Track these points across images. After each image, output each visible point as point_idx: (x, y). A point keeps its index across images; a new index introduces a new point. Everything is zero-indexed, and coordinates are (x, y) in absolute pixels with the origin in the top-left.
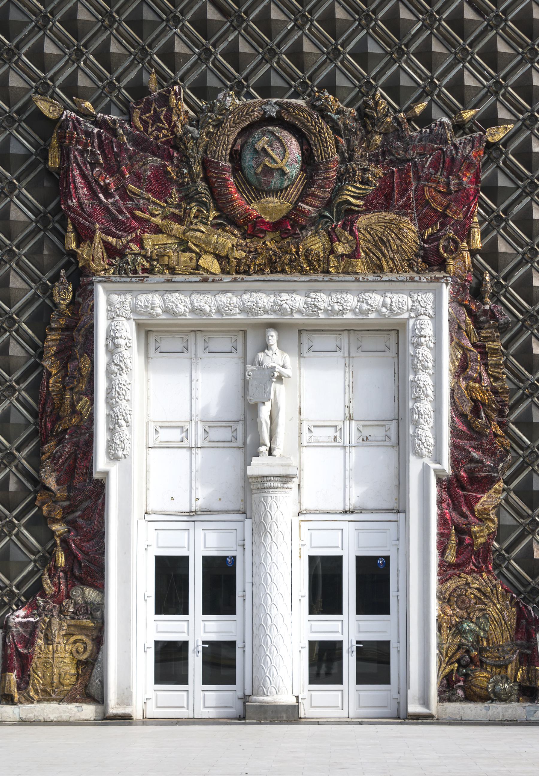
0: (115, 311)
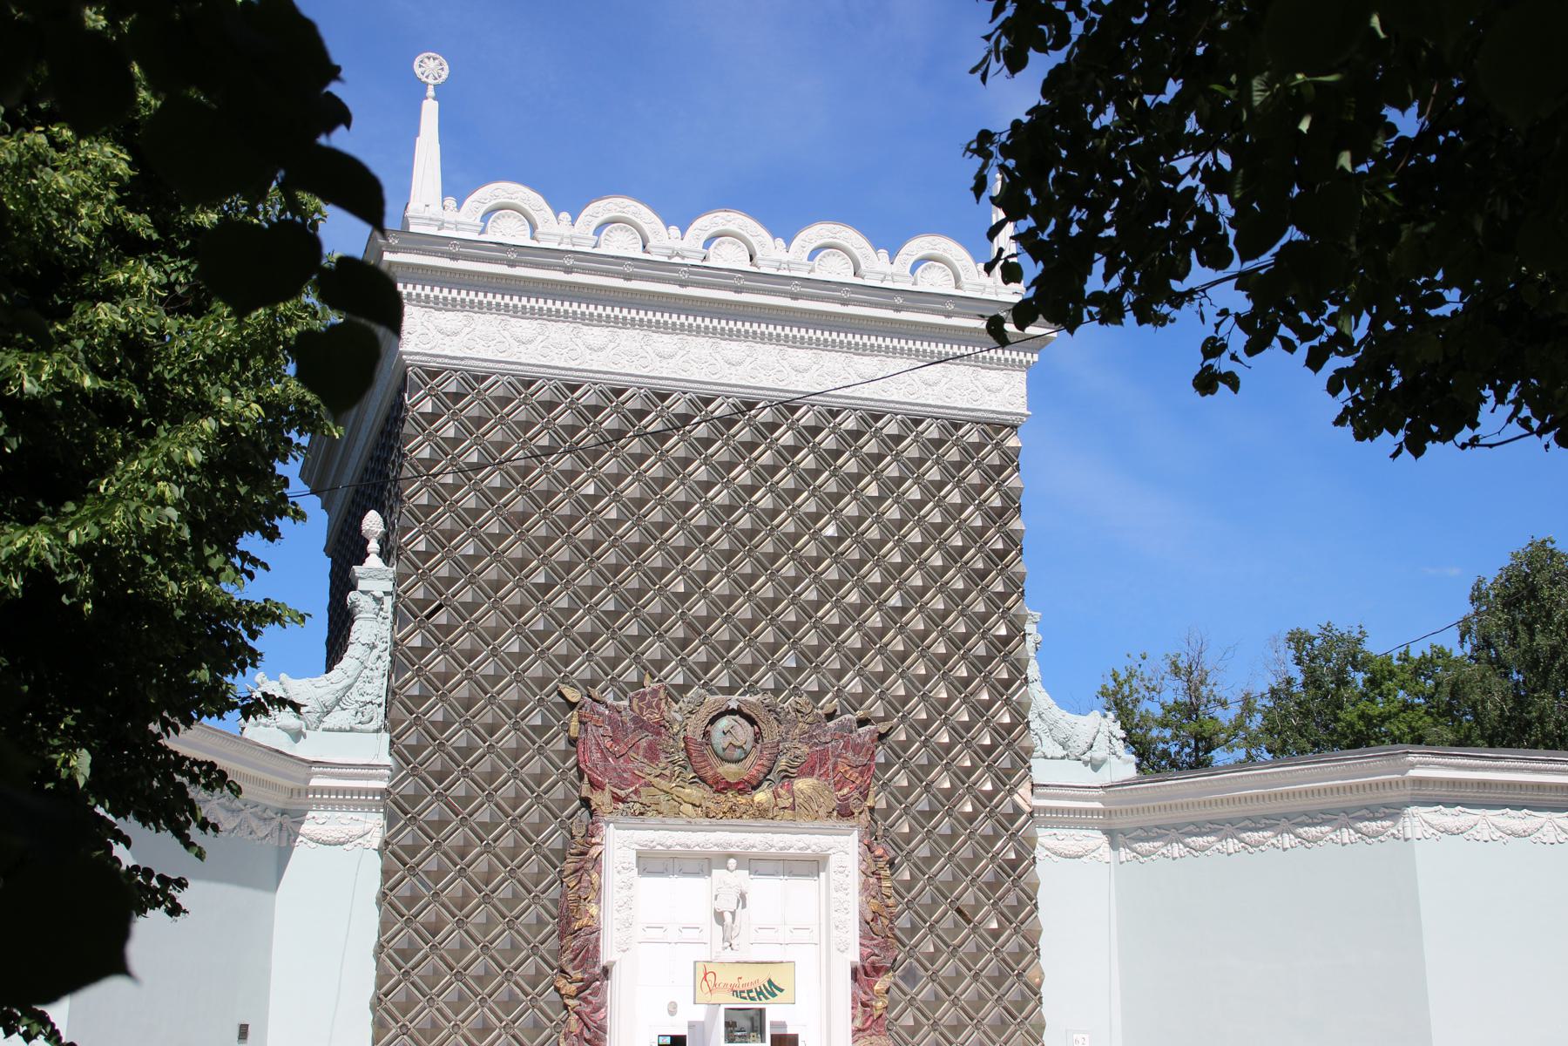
0: (619, 844)
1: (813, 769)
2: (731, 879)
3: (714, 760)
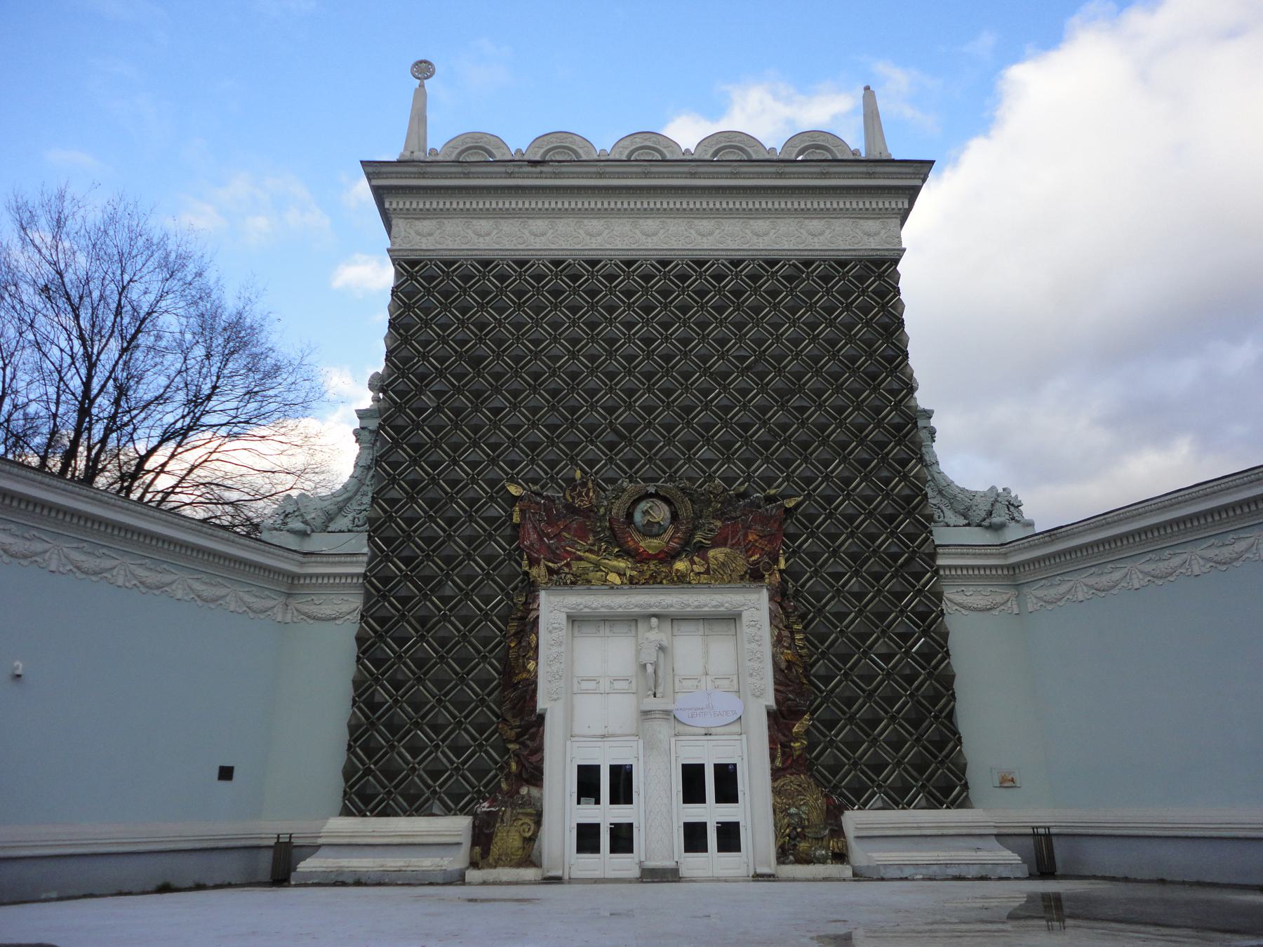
0: (552, 608)
1: (726, 539)
2: (655, 635)
3: (637, 537)
